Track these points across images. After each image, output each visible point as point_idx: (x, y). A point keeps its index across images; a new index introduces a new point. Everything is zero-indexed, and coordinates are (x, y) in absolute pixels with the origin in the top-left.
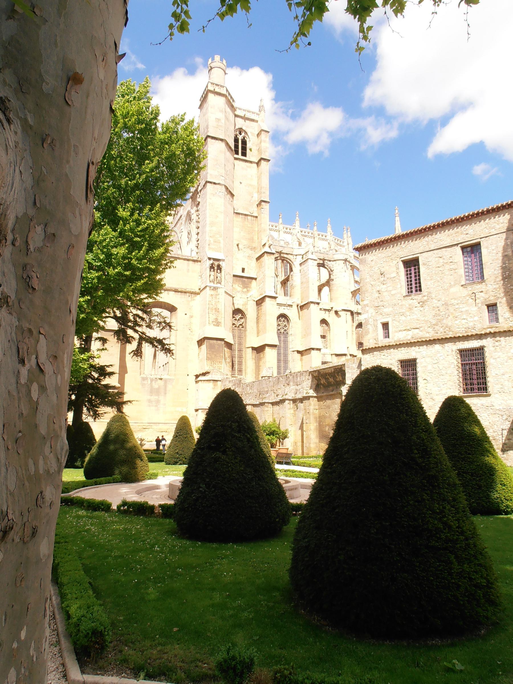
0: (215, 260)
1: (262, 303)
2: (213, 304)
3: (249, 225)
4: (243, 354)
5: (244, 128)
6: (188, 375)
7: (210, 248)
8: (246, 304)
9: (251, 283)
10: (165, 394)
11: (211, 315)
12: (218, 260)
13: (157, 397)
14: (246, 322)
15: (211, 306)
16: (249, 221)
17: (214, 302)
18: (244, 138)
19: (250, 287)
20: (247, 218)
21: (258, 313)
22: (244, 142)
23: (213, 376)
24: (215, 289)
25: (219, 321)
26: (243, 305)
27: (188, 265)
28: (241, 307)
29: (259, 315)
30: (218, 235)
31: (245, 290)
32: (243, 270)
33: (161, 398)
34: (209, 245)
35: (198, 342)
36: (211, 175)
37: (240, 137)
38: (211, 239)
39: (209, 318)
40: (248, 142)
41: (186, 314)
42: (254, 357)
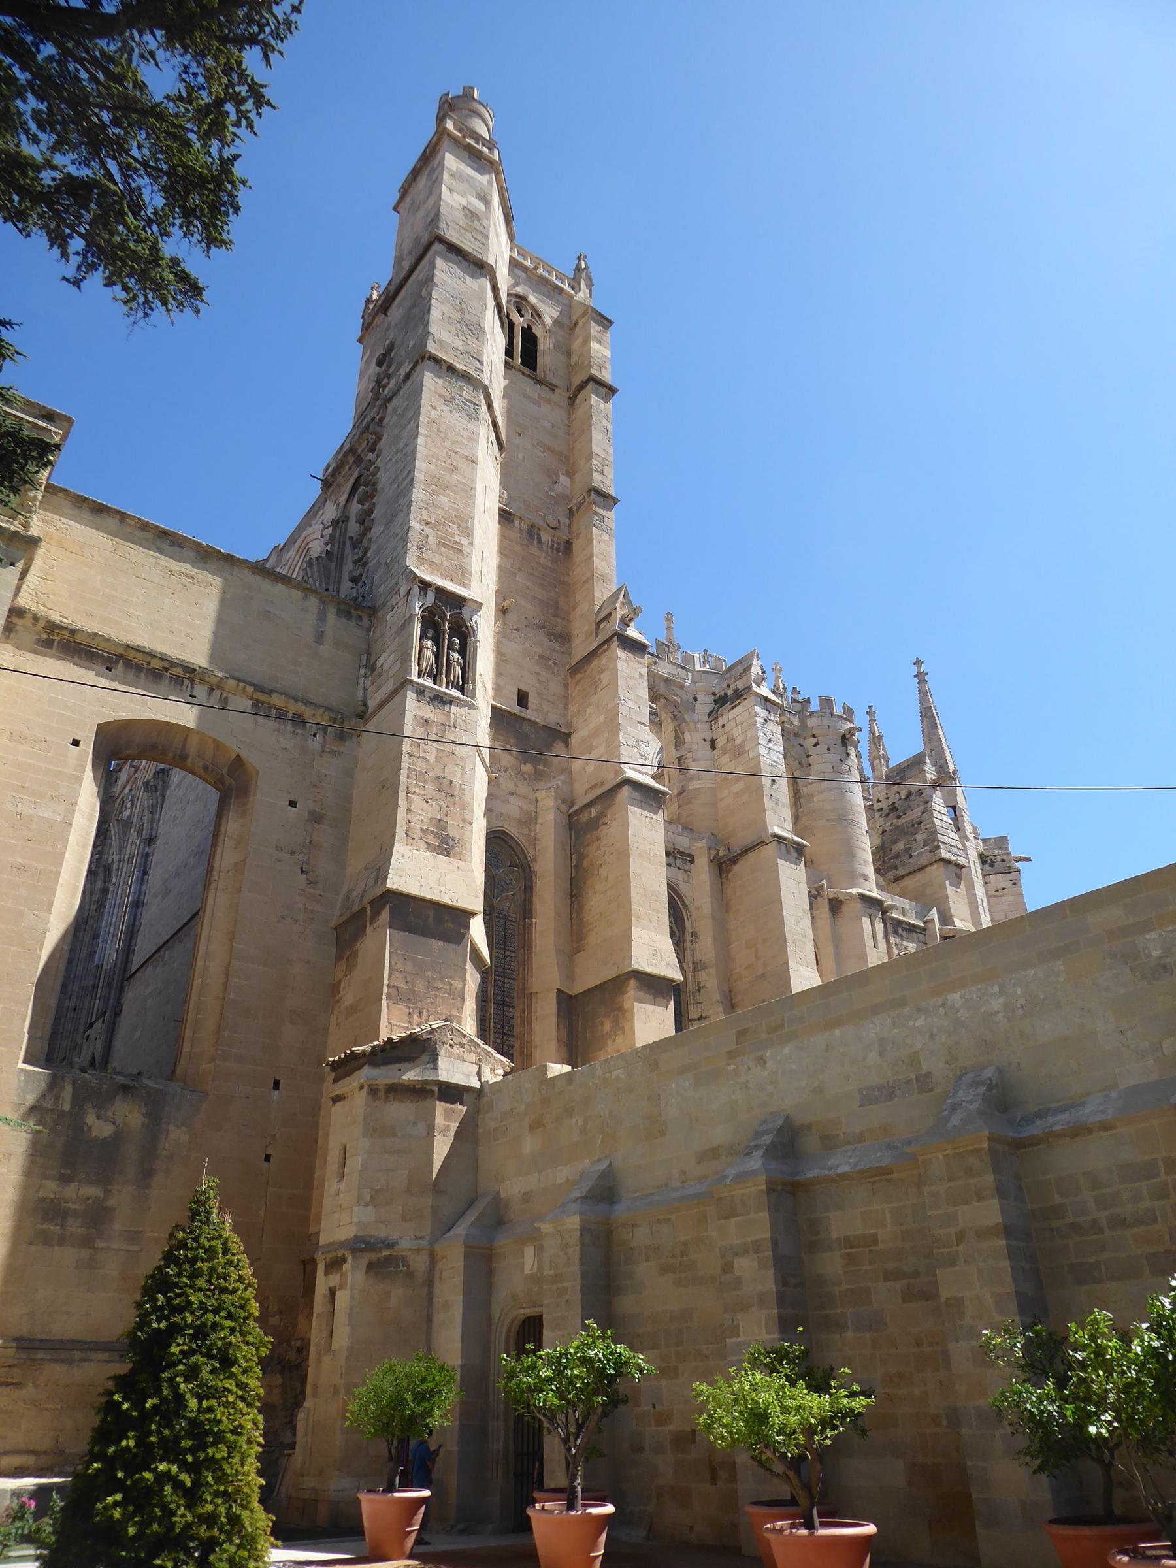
0: (440, 591)
1: (602, 814)
2: (432, 759)
3: (542, 561)
4: (516, 1022)
5: (533, 299)
6: (276, 1084)
7: (422, 561)
8: (530, 819)
9: (549, 746)
10: (146, 1174)
11: (417, 801)
12: (458, 602)
13: (95, 1192)
14: (529, 889)
15: (421, 766)
16: (544, 547)
17: (435, 753)
18: (529, 327)
19: (546, 764)
20: (540, 541)
21: (581, 857)
22: (529, 338)
23: (442, 1063)
24: (439, 700)
25: (452, 832)
26: (521, 823)
27: (322, 617)
28: (512, 830)
29: (585, 863)
30: (455, 526)
31: (527, 768)
32: (523, 699)
33: (122, 1197)
34: (420, 548)
35: (338, 930)
36: (440, 343)
37: (519, 321)
38: (428, 530)
39: (409, 811)
40: (540, 341)
41: (293, 804)
42: (564, 1035)
